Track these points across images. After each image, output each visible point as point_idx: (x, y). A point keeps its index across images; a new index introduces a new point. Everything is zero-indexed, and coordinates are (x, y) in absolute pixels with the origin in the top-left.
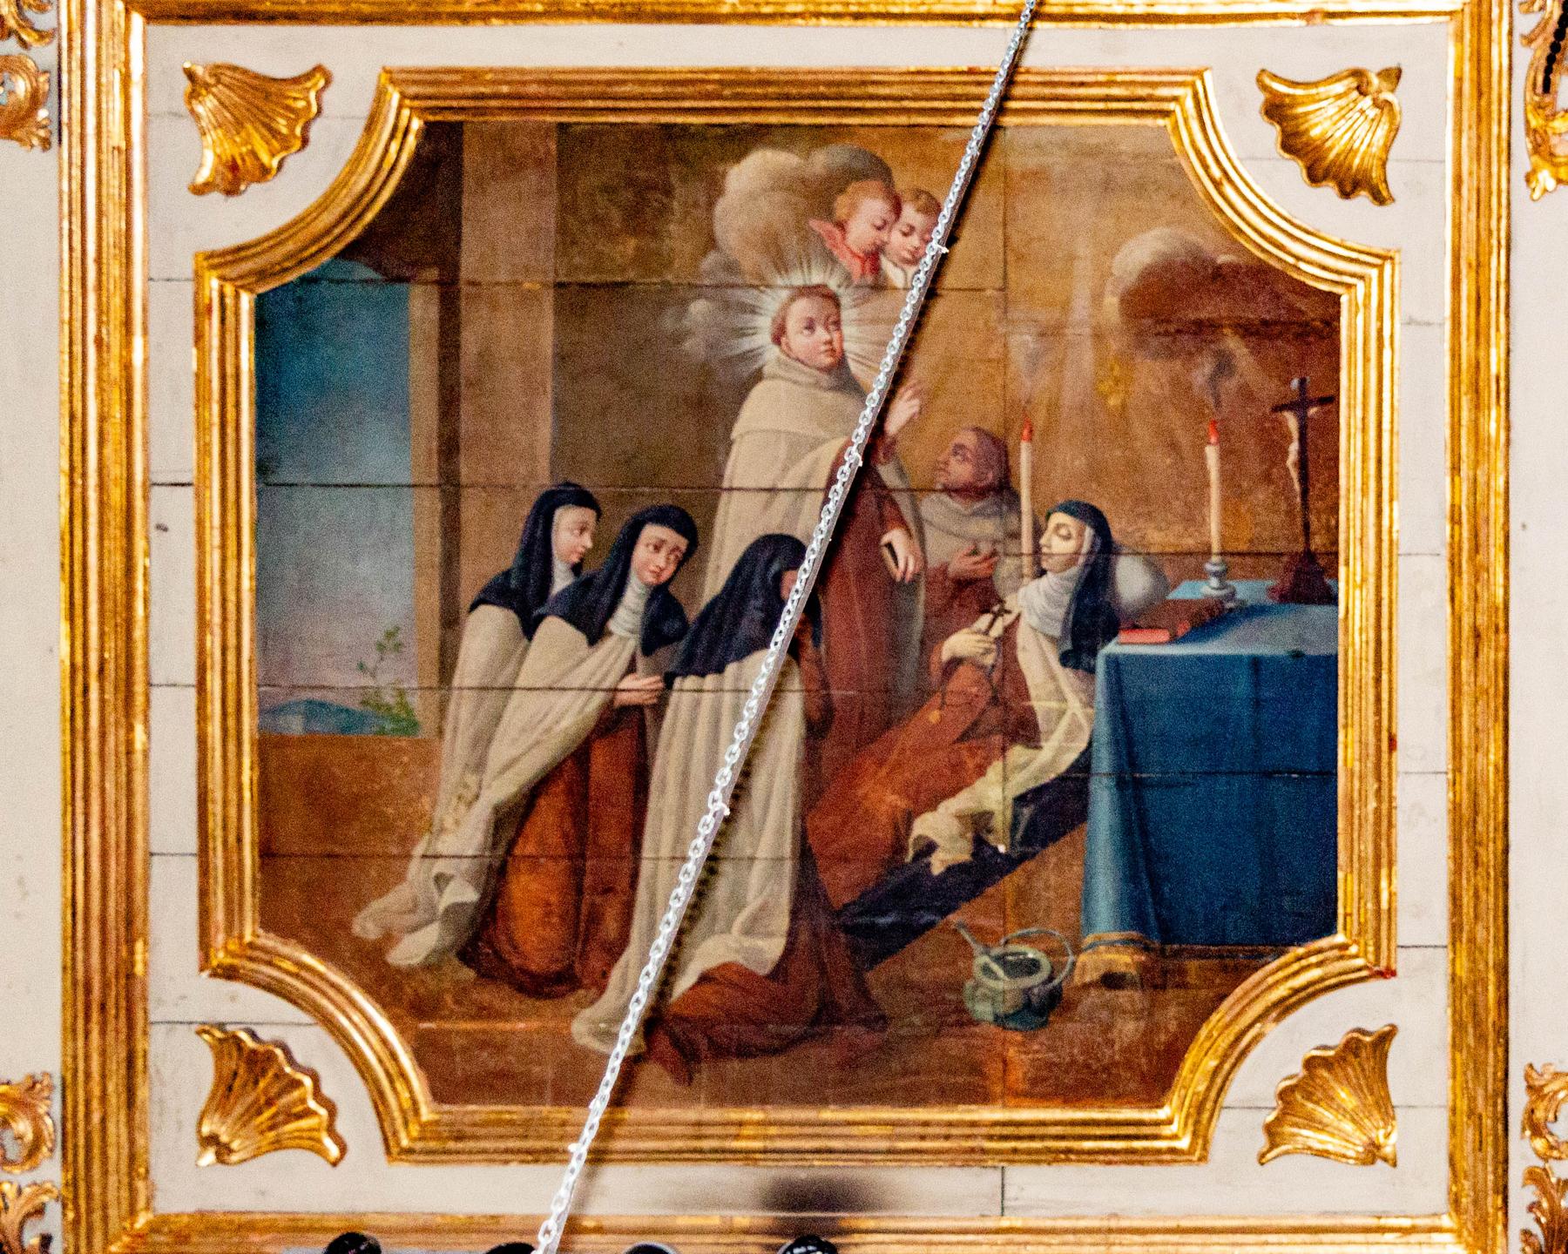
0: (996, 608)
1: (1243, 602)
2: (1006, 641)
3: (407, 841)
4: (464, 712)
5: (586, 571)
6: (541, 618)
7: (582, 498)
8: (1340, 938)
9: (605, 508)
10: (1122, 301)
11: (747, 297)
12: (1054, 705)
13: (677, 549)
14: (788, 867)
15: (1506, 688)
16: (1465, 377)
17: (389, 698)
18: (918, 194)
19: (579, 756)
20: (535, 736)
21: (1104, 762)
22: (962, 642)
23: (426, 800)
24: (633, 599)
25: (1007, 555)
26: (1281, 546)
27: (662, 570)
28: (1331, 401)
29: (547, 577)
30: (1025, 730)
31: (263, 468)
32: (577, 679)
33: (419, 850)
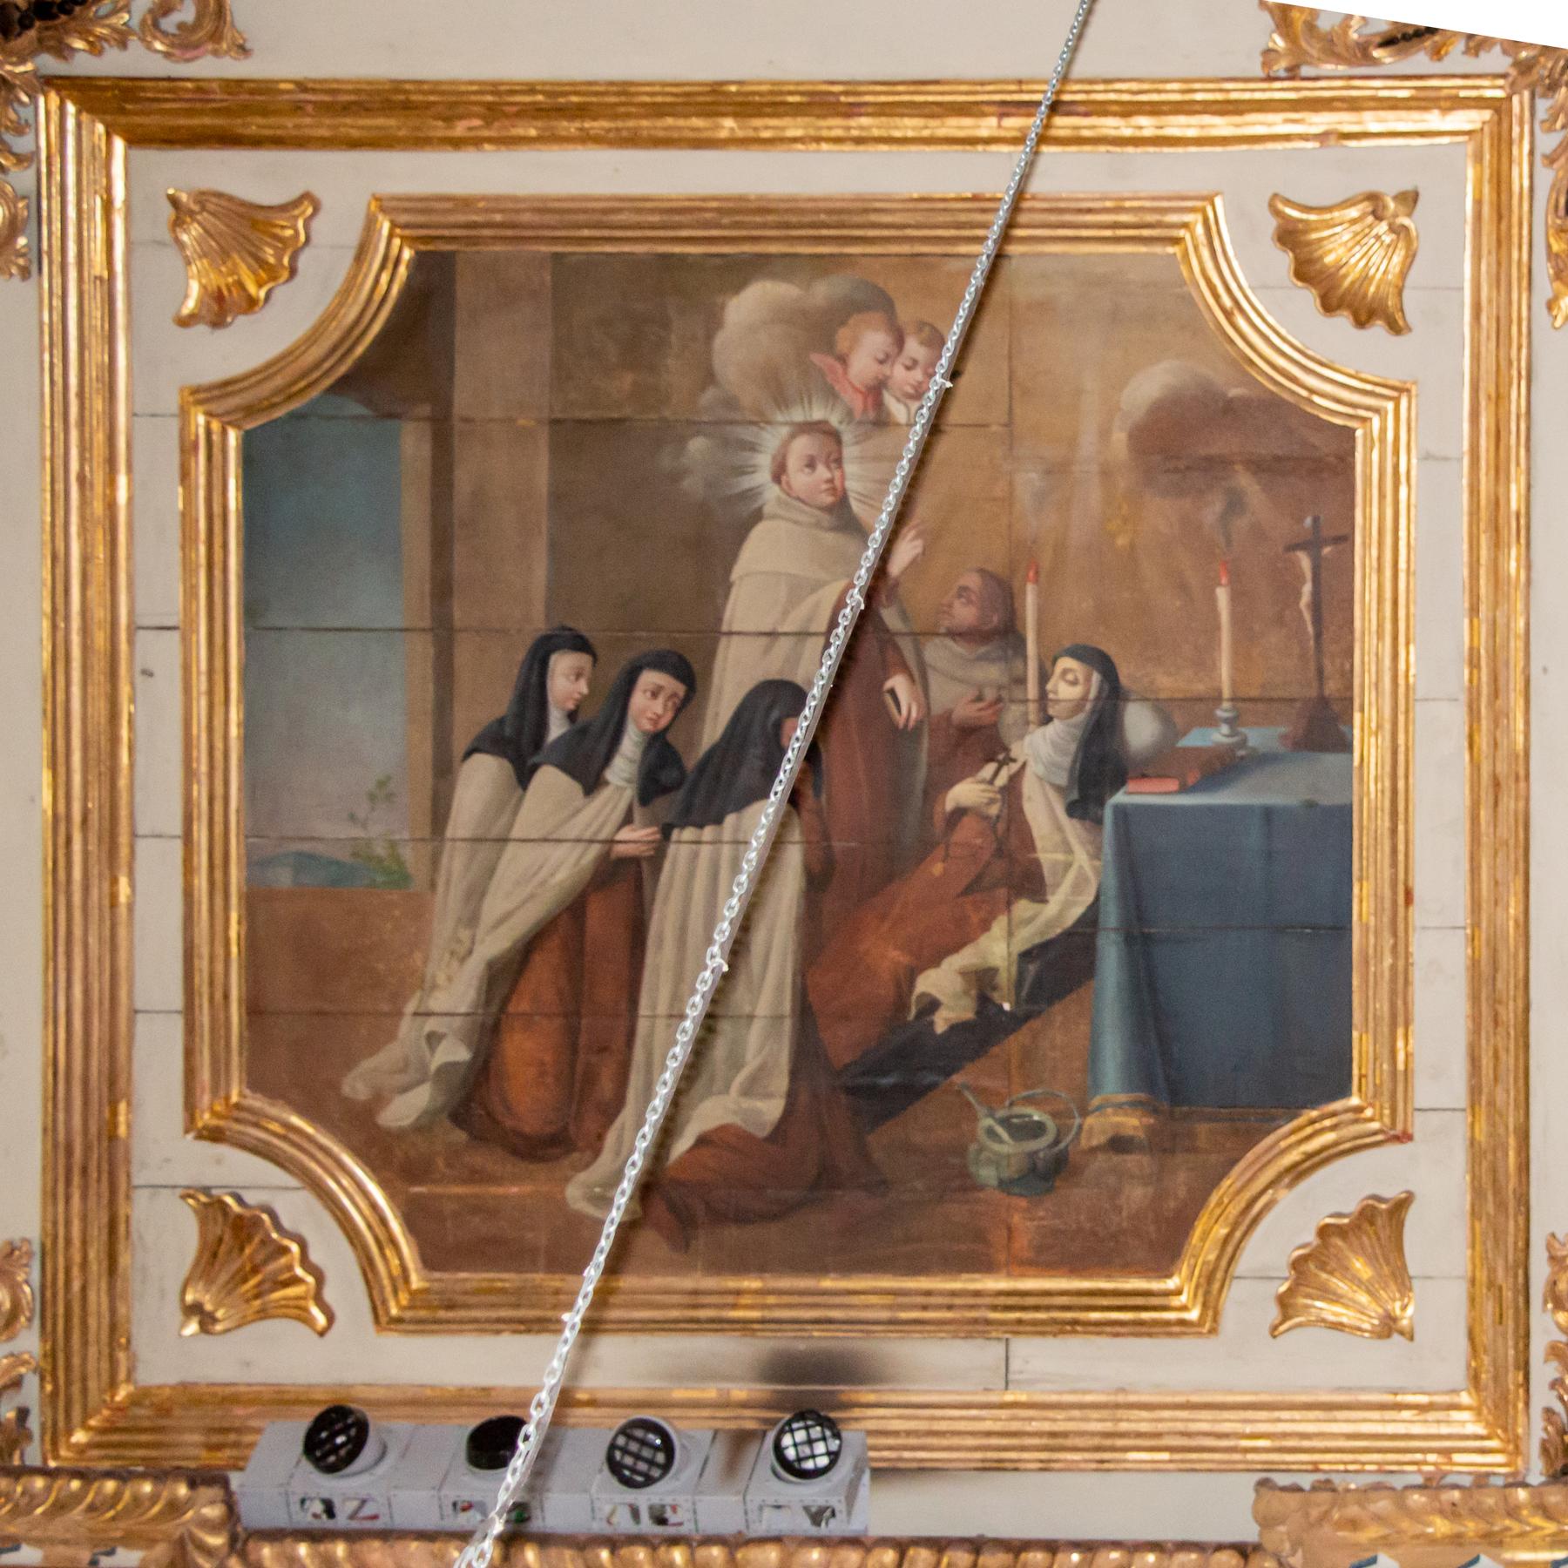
0: (1001, 757)
1: (1254, 749)
2: (1012, 792)
3: (398, 999)
4: (456, 864)
5: (582, 718)
6: (534, 769)
7: (580, 644)
8: (1355, 1101)
9: (600, 652)
10: (1131, 436)
11: (746, 433)
12: (1060, 857)
13: (674, 695)
14: (787, 1025)
15: (1527, 839)
16: (1484, 514)
17: (380, 850)
18: (921, 325)
19: (574, 909)
20: (528, 890)
21: (1111, 916)
22: (965, 792)
23: (418, 956)
24: (630, 746)
25: (1012, 701)
26: (1294, 691)
27: (659, 717)
28: (1345, 539)
29: (542, 725)
30: (1031, 884)
31: (252, 611)
32: (573, 829)
33: (410, 1007)
